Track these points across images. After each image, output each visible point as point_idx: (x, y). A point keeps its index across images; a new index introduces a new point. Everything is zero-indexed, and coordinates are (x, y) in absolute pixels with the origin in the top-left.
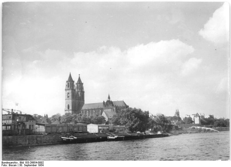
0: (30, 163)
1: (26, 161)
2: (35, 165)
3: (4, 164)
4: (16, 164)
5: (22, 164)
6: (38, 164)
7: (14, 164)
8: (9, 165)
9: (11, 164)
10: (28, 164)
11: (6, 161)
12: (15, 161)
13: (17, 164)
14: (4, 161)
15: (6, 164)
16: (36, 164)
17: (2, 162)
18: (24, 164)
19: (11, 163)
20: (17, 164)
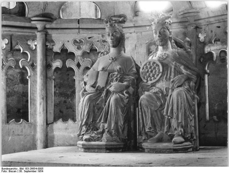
0: (30, 169)
1: (26, 167)
2: (35, 171)
3: (4, 170)
4: (16, 170)
5: (22, 170)
6: (37, 170)
7: (14, 170)
8: (9, 171)
9: (11, 170)
10: (27, 170)
11: (6, 167)
12: (15, 167)
14: (4, 167)
15: (6, 170)
16: (36, 170)
17: (2, 169)
19: (11, 169)
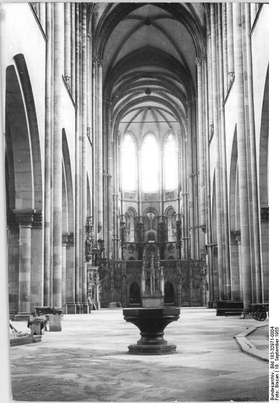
2: (277, 342)
3: (275, 396)
4: (275, 375)
5: (275, 364)
8: (277, 386)
9: (275, 383)
10: (275, 355)
11: (270, 393)
12: (270, 377)
13: (275, 374)
14: (270, 396)
15: (275, 393)
17: (272, 399)
18: (275, 362)
19: (273, 383)
20: (275, 374)
